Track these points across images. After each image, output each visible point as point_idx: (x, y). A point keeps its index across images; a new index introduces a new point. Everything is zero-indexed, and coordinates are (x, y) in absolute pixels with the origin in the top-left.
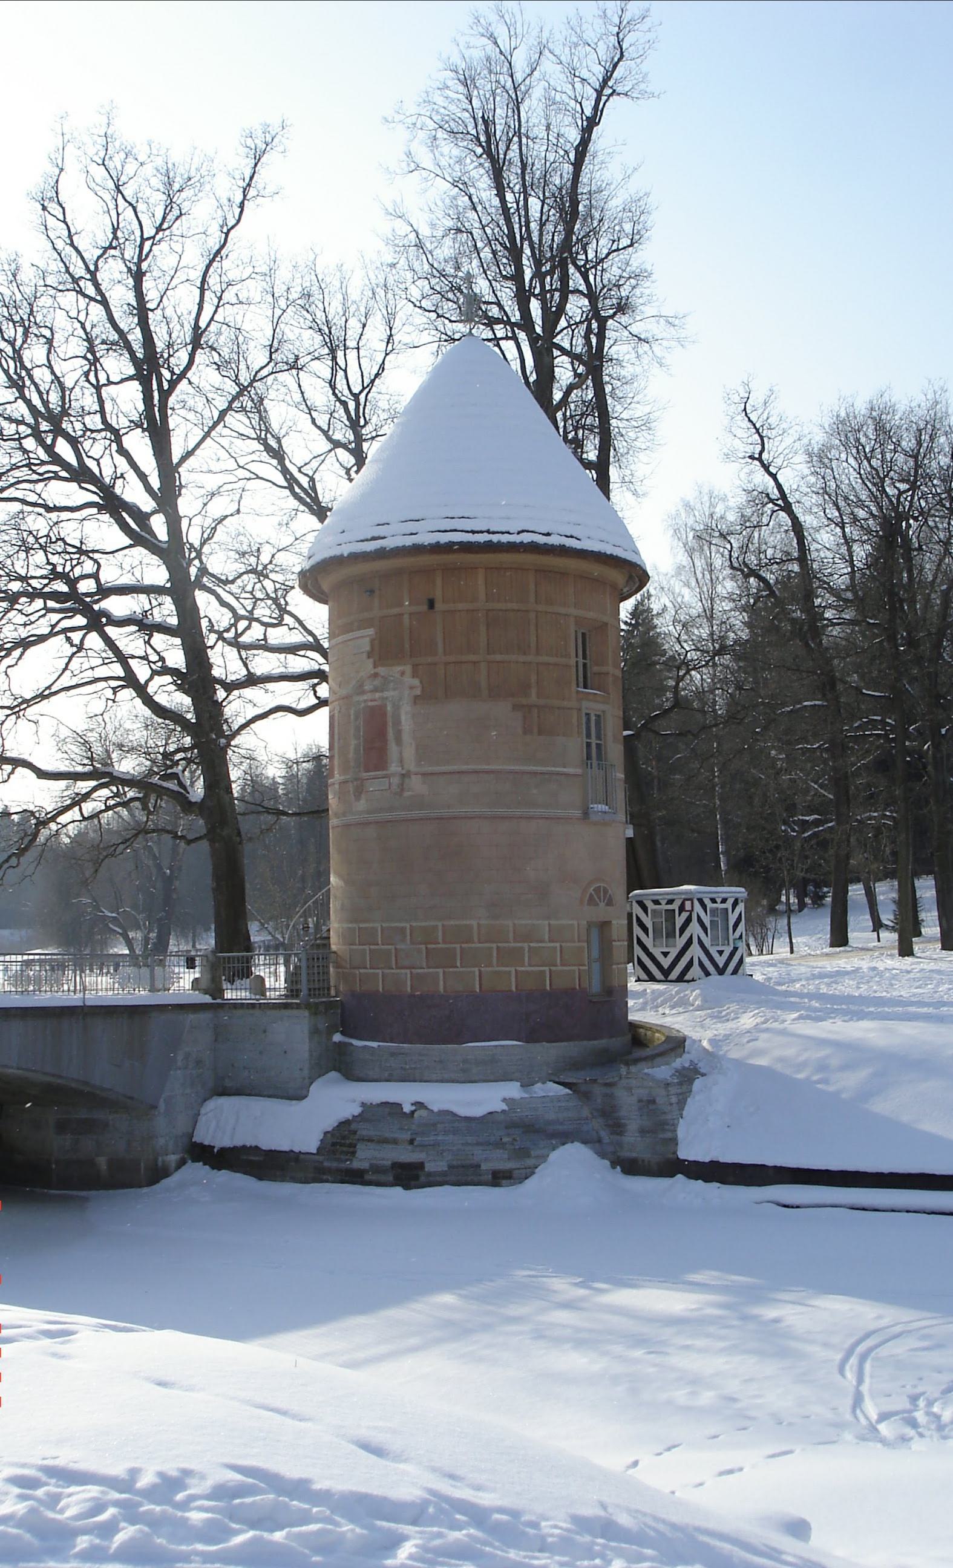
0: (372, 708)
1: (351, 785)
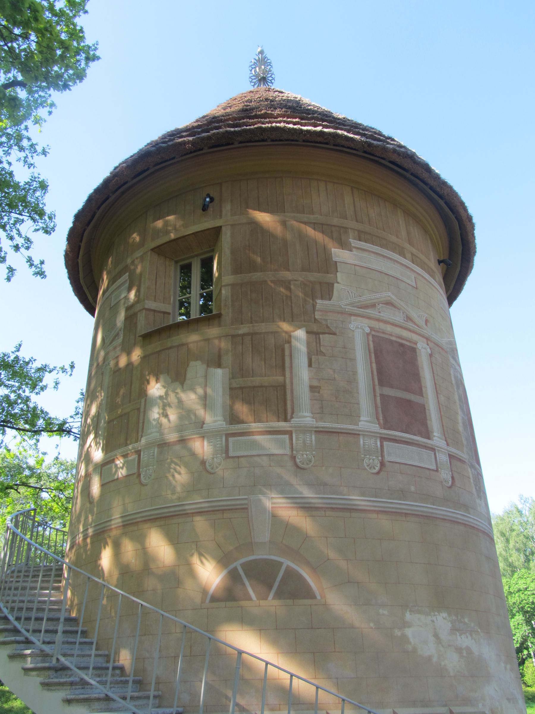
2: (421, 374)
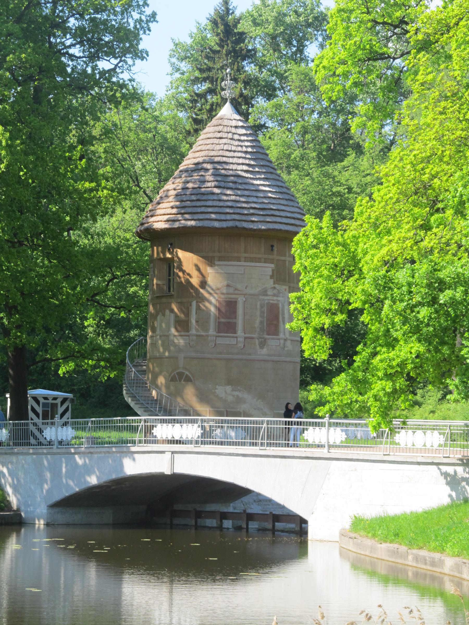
0: (272, 304)
1: (257, 340)
2: (237, 311)
